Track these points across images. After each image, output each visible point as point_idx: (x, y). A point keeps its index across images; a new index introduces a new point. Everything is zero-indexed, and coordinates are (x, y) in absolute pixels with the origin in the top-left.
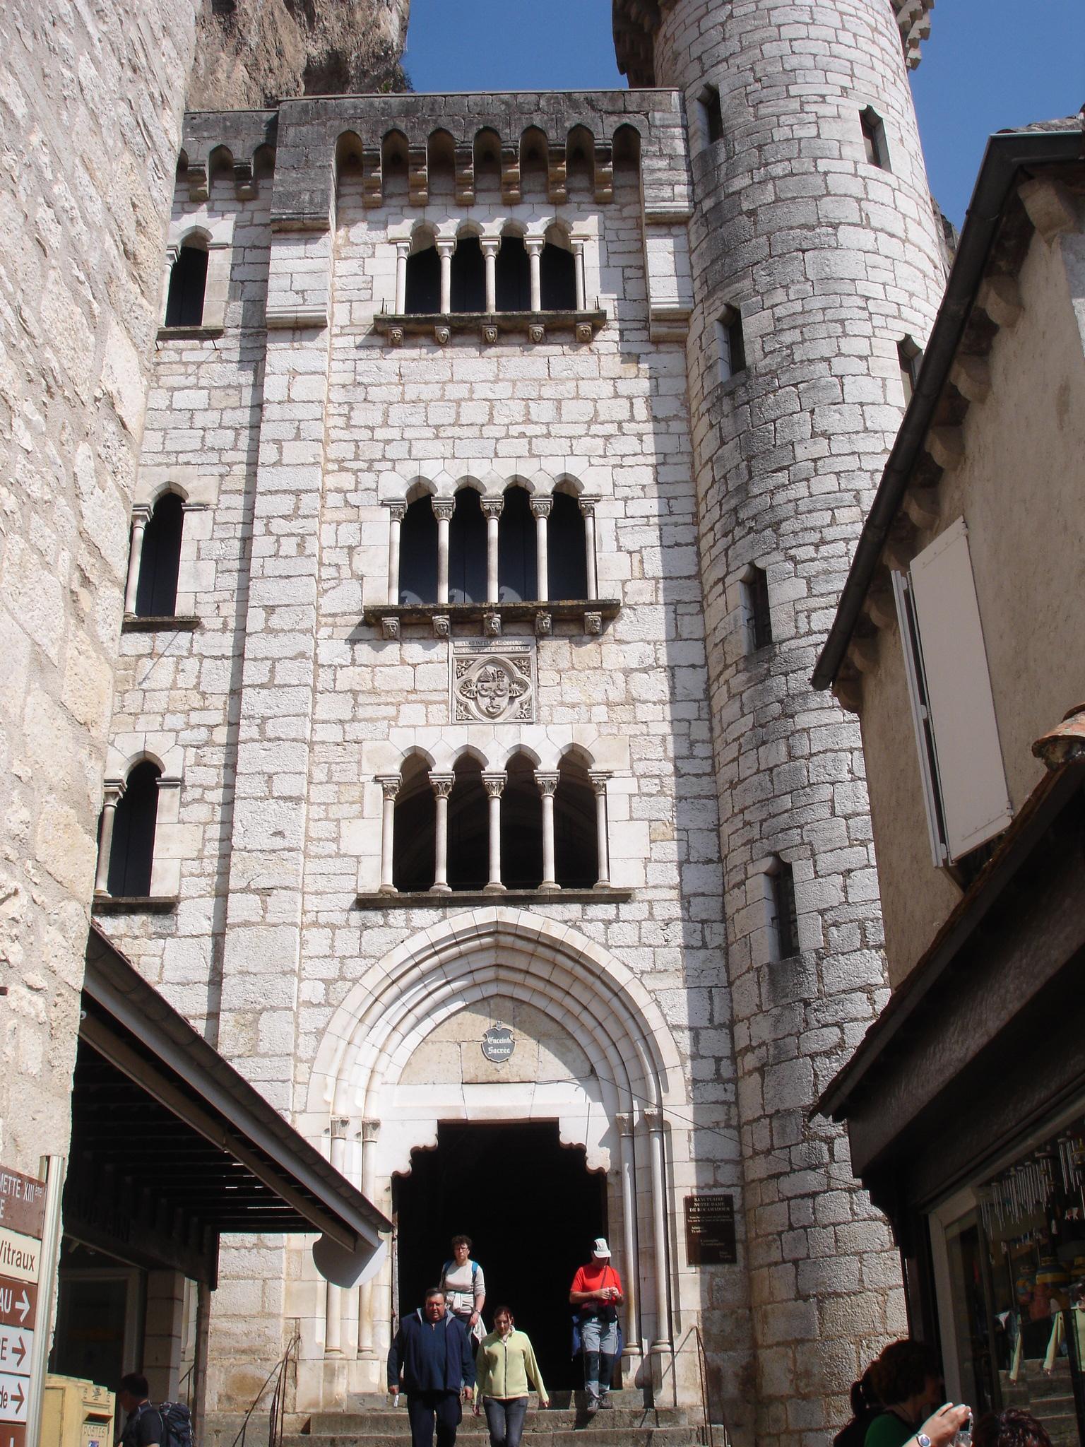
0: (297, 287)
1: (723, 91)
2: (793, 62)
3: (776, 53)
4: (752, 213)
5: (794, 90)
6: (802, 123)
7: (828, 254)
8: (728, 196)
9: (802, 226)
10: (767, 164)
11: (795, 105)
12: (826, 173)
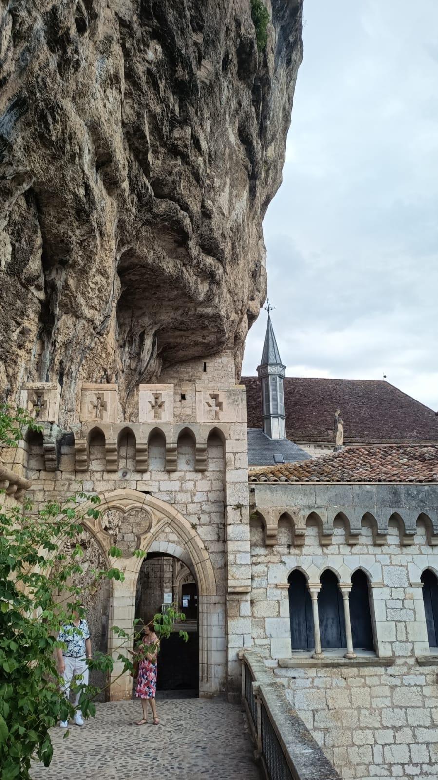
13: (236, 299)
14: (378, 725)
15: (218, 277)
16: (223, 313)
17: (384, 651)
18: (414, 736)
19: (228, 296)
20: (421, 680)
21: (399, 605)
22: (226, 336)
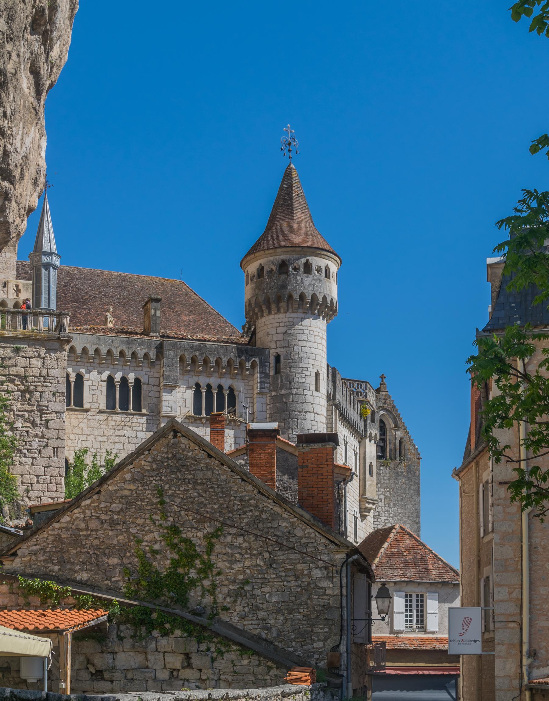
0: (170, 406)
1: (282, 358)
2: (301, 355)
3: (297, 350)
4: (286, 403)
5: (301, 365)
6: (302, 377)
7: (303, 421)
8: (280, 394)
9: (298, 411)
10: (291, 389)
11: (300, 371)
12: (305, 395)
13: (20, 207)
14: (80, 433)
15: (10, 195)
16: (11, 220)
17: (86, 406)
18: (95, 438)
19: (15, 205)
20: (101, 418)
21: (95, 388)
22: (11, 237)
